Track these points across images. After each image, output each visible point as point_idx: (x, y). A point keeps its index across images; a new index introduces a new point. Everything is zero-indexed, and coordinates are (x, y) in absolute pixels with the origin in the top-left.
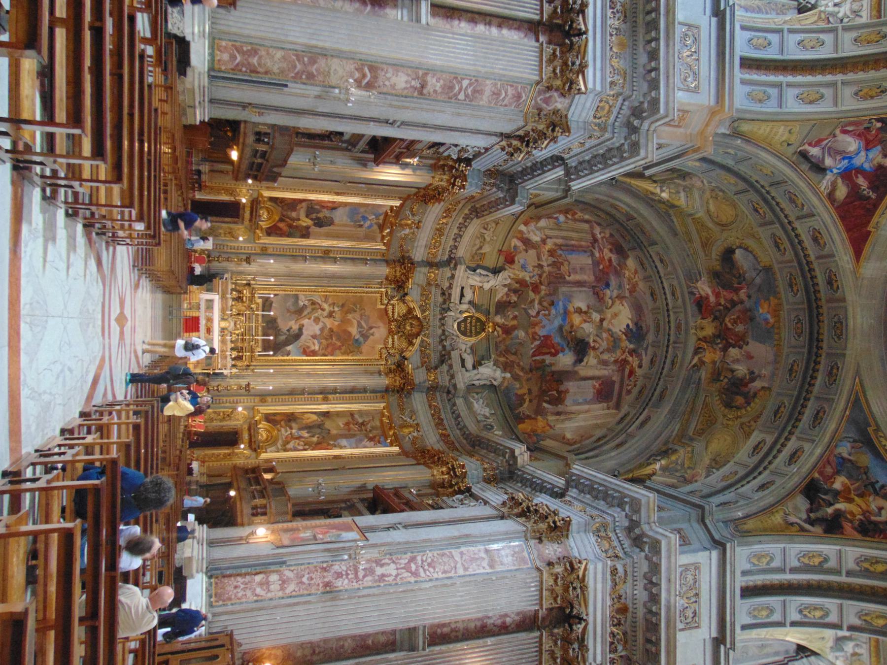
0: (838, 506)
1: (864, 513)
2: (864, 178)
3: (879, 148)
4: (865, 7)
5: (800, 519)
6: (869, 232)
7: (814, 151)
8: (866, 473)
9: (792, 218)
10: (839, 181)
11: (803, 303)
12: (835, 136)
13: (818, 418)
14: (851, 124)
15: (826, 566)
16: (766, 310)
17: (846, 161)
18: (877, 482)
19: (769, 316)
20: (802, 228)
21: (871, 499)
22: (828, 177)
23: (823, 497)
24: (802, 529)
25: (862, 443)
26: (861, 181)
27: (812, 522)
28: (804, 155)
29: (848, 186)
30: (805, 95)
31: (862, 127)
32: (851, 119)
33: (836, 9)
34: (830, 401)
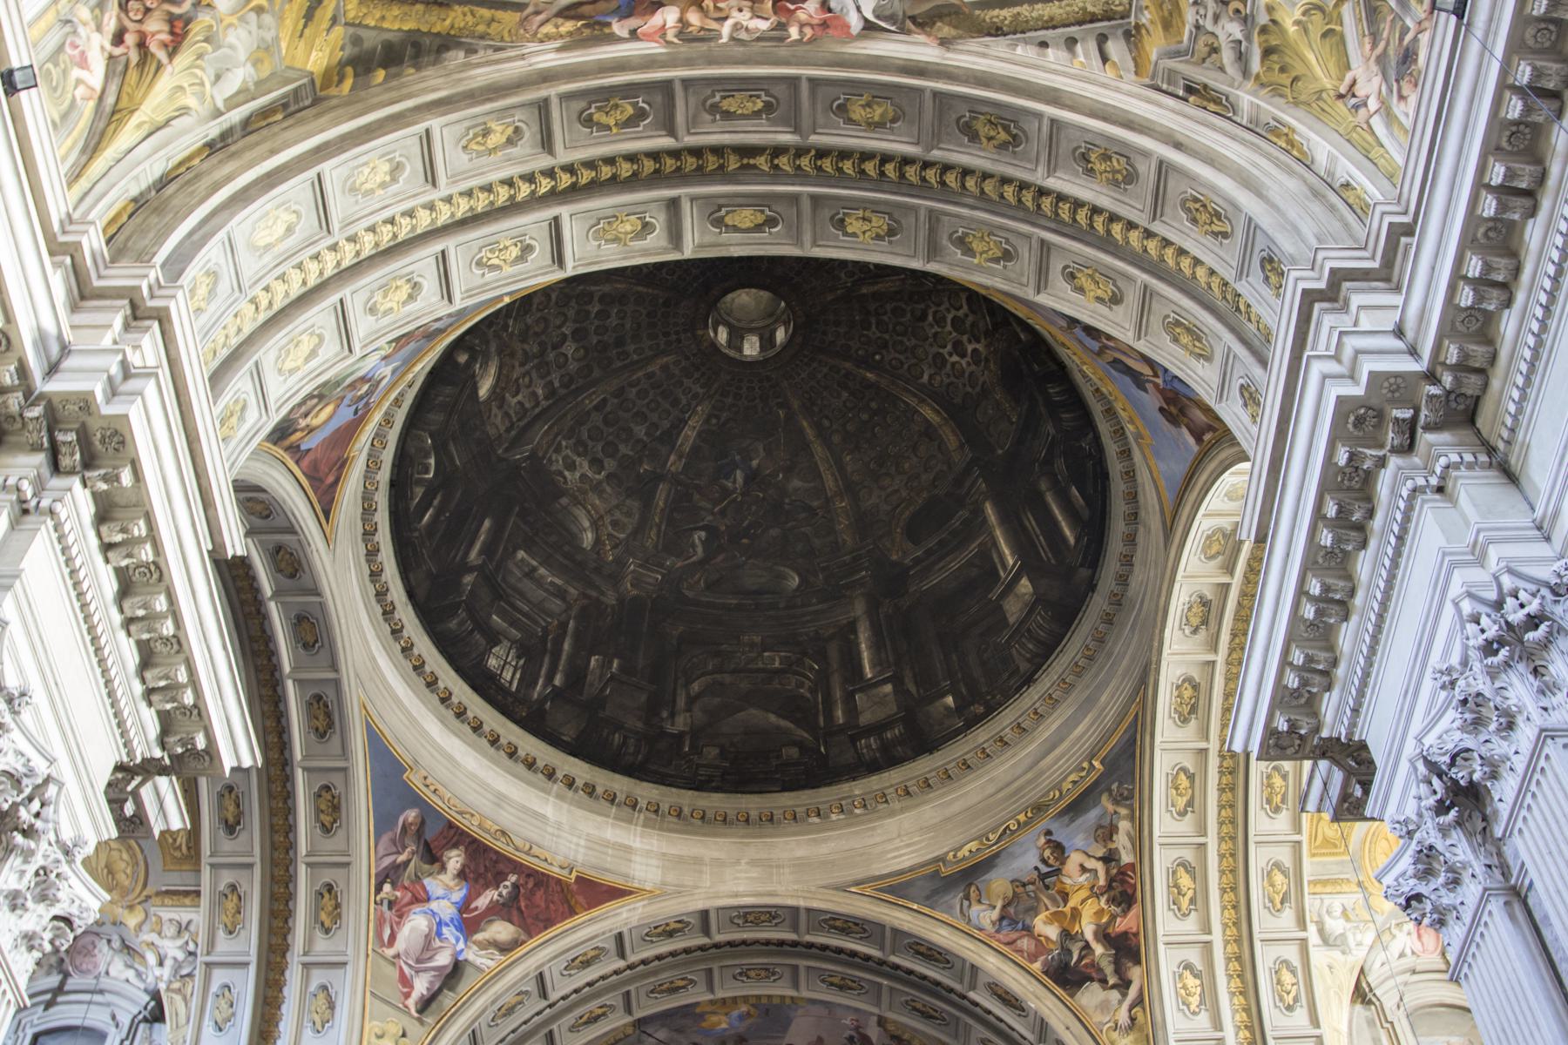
0: (1088, 929)
1: (1095, 893)
2: (479, 895)
3: (427, 881)
4: (177, 918)
5: (1120, 1002)
6: (581, 880)
7: (421, 986)
8: (1024, 885)
9: (545, 1003)
10: (479, 937)
11: (709, 972)
12: (398, 956)
13: (932, 953)
14: (379, 934)
15: (1199, 966)
16: (723, 1018)
17: (445, 930)
18: (1036, 868)
19: (735, 1013)
20: (560, 987)
21: (1068, 881)
22: (472, 955)
23: (1075, 958)
24: (1139, 1001)
25: (971, 884)
26: (482, 902)
27: (1124, 985)
28: (426, 1004)
29: (491, 922)
30: (317, 1018)
31: (388, 914)
32: (371, 934)
33: (169, 963)
34: (897, 932)
